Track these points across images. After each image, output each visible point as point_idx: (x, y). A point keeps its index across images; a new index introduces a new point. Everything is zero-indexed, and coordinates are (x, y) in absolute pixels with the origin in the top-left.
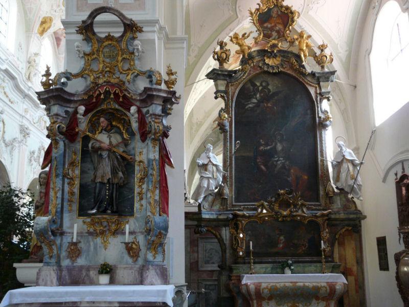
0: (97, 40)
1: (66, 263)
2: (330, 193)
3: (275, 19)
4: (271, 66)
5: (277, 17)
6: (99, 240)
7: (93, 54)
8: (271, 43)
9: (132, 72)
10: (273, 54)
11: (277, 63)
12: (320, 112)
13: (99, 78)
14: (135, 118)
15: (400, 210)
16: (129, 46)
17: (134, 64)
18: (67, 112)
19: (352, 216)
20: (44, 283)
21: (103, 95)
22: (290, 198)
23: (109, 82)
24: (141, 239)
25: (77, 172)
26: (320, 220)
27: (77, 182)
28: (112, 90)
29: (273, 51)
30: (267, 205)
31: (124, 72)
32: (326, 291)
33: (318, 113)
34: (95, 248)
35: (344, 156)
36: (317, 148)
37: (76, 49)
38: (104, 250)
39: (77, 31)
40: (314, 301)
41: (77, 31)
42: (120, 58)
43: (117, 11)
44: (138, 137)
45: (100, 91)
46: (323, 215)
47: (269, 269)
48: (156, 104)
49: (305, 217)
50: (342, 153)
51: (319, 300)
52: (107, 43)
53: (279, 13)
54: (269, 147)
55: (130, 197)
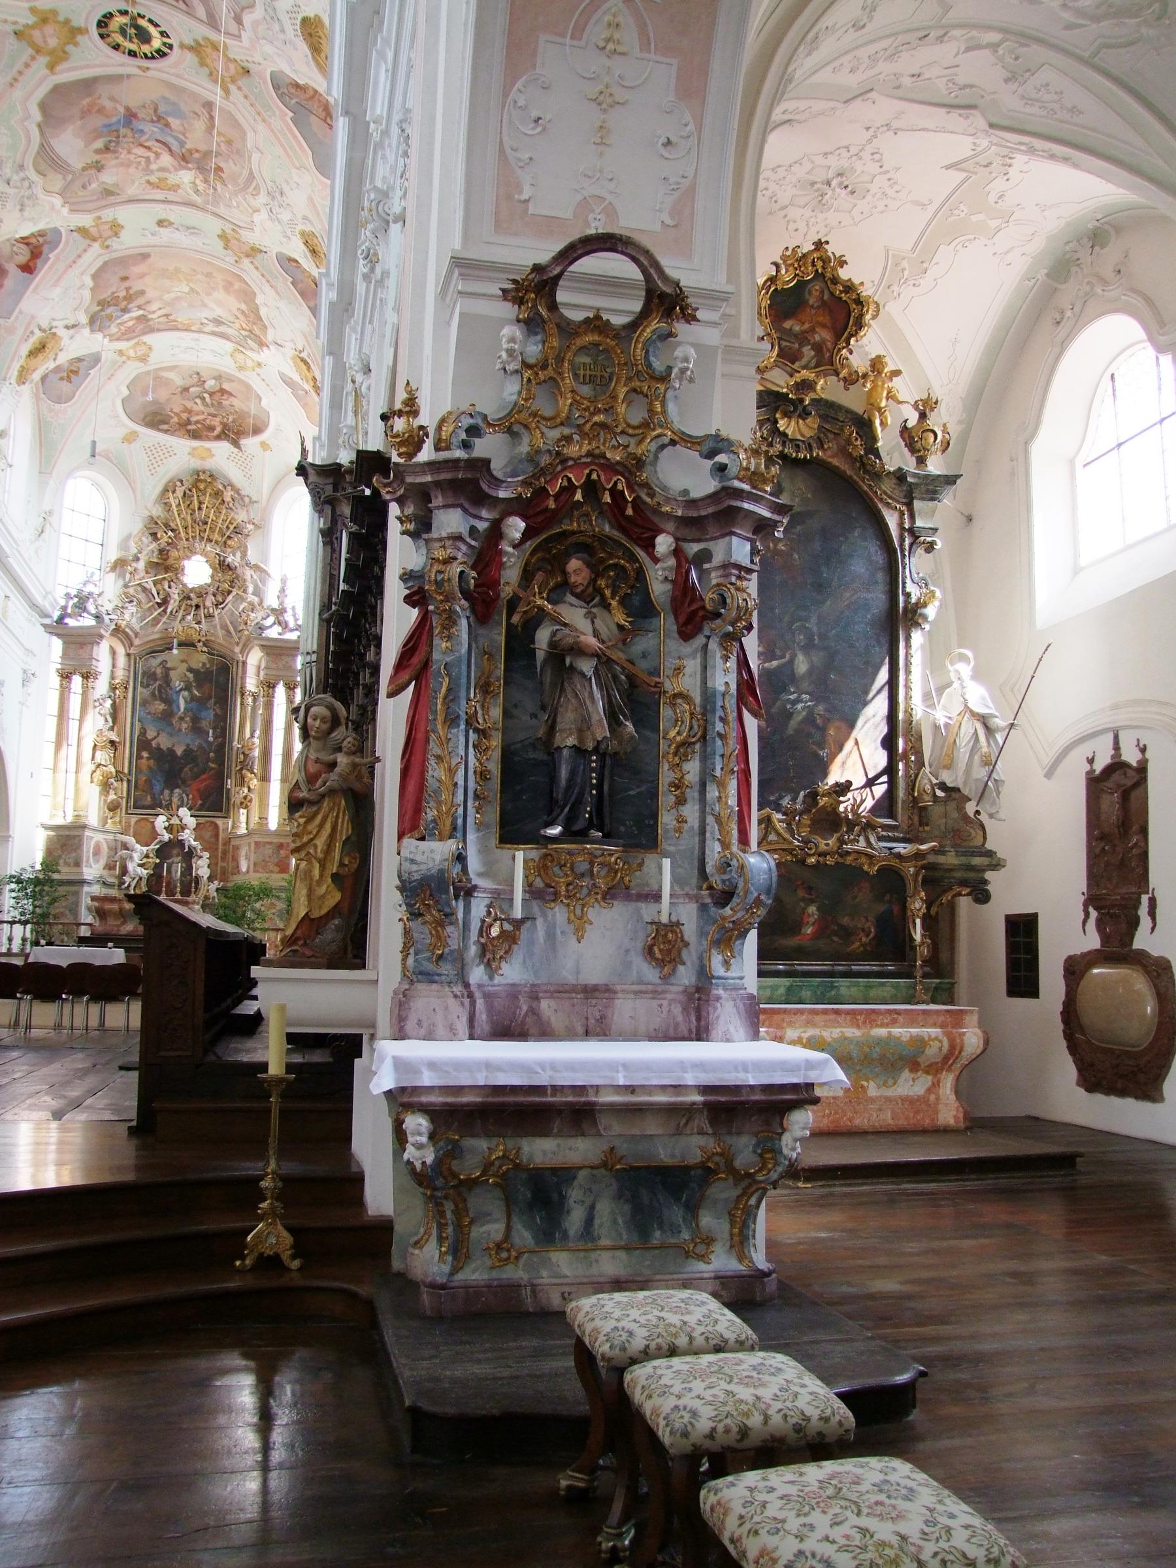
0: (558, 326)
1: (477, 974)
3: (813, 311)
4: (791, 440)
5: (819, 307)
6: (559, 914)
7: (544, 367)
8: (798, 377)
9: (654, 433)
10: (800, 408)
11: (808, 433)
13: (568, 439)
14: (664, 569)
15: (1098, 851)
16: (652, 359)
17: (664, 412)
18: (473, 530)
20: (423, 1032)
21: (579, 491)
23: (603, 456)
24: (688, 916)
25: (496, 713)
27: (496, 742)
28: (609, 481)
29: (802, 401)
30: (780, 821)
31: (631, 431)
32: (940, 1049)
34: (551, 935)
37: (505, 346)
38: (574, 940)
39: (504, 291)
40: (906, 1074)
41: (504, 291)
42: (622, 391)
43: (647, 252)
44: (666, 622)
45: (569, 480)
47: (782, 991)
48: (738, 535)
51: (917, 1071)
52: (588, 338)
53: (826, 297)
54: (775, 663)
55: (631, 793)
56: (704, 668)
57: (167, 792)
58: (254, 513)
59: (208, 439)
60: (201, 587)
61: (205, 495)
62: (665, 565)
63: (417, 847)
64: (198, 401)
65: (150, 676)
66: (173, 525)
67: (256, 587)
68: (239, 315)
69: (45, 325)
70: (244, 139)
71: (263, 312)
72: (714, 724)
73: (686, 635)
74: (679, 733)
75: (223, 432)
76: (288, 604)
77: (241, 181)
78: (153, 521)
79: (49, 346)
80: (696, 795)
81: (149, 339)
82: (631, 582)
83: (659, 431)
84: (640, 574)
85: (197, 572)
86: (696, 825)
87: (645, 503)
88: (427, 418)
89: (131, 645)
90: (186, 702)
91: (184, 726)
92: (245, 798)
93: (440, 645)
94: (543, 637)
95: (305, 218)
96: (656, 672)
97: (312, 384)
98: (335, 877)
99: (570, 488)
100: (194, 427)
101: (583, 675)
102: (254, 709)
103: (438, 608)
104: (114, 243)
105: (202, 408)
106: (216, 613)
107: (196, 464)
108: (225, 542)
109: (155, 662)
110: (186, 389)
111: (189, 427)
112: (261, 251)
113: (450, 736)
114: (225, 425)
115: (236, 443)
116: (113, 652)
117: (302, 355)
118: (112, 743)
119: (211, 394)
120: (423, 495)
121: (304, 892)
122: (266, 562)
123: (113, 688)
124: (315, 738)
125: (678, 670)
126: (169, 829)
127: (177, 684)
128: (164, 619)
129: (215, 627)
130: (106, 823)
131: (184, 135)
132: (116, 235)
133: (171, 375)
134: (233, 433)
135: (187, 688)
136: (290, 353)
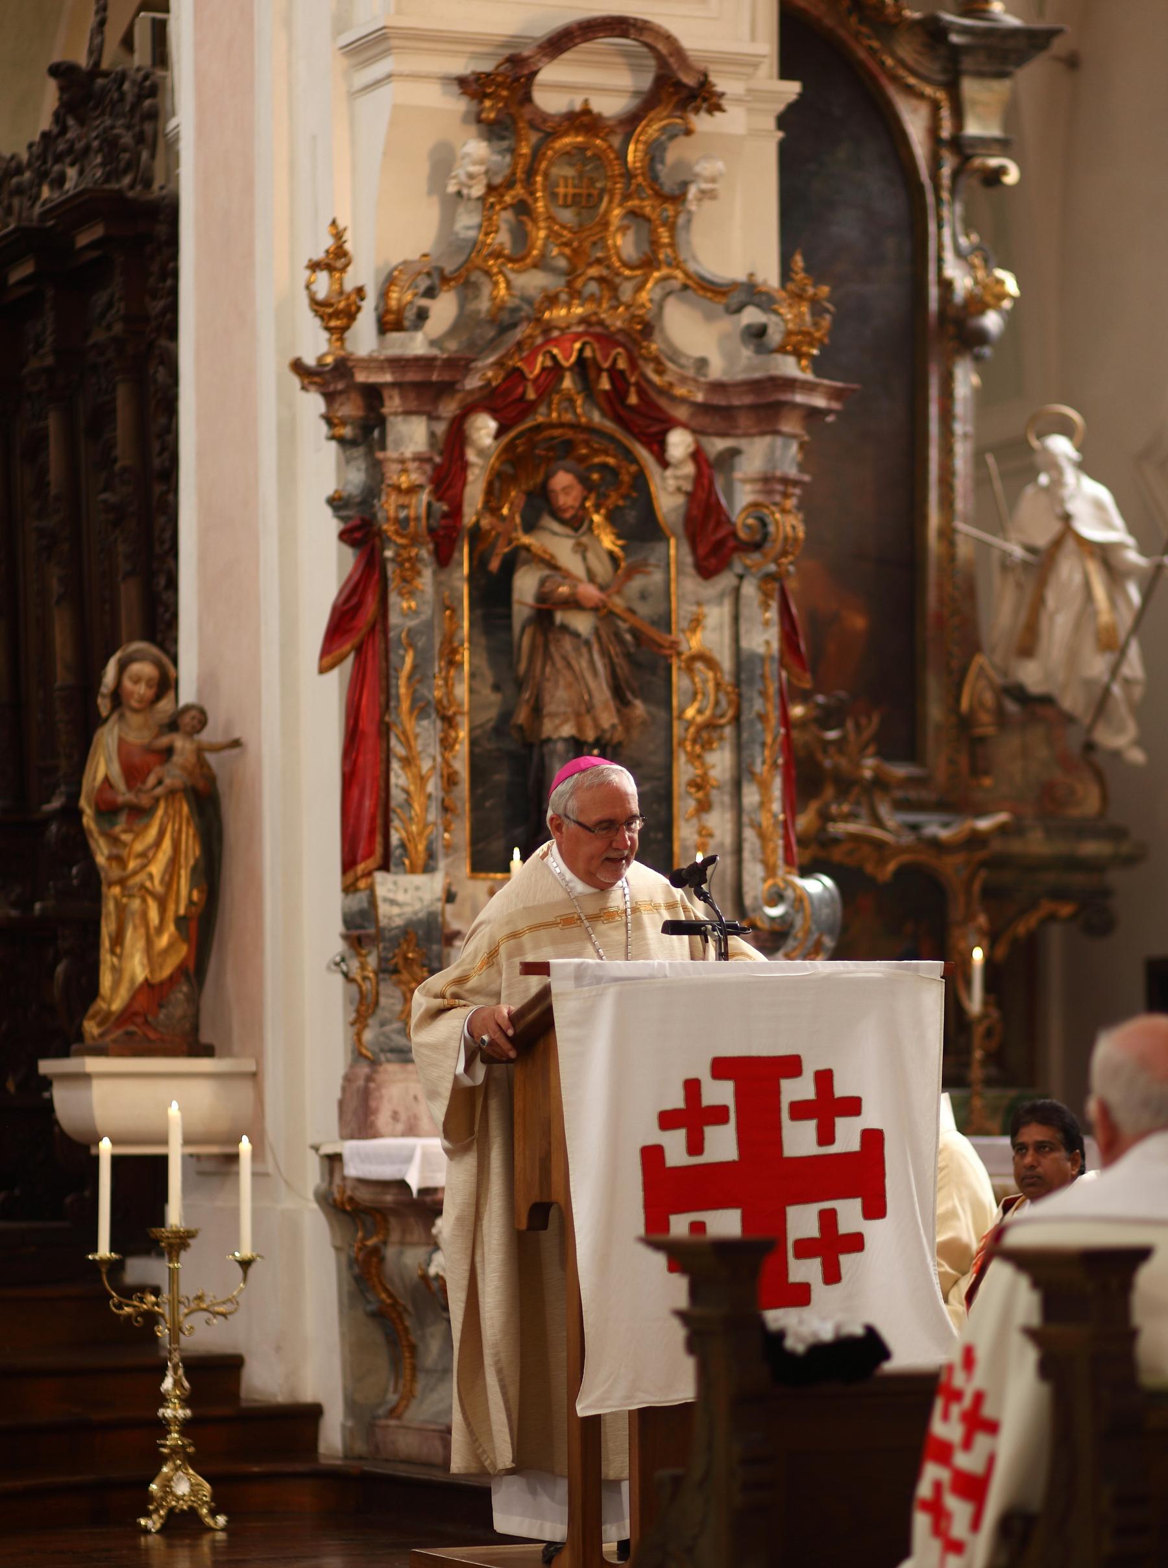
2: (985, 718)
12: (949, 255)
14: (677, 478)
17: (672, 245)
19: (1091, 848)
20: (400, 1127)
22: (826, 744)
26: (951, 867)
28: (606, 357)
33: (940, 260)
35: (1067, 518)
36: (925, 460)
44: (677, 550)
45: (554, 357)
46: (975, 840)
49: (879, 845)
50: (1061, 501)
56: (736, 619)
62: (680, 472)
63: (395, 883)
72: (751, 700)
73: (707, 570)
74: (700, 711)
80: (727, 799)
82: (624, 490)
83: (665, 271)
84: (641, 482)
86: (728, 840)
87: (649, 381)
88: (362, 273)
93: (399, 604)
94: (526, 585)
96: (665, 622)
98: (180, 921)
99: (555, 371)
101: (576, 635)
103: (397, 555)
113: (418, 730)
120: (373, 395)
121: (141, 944)
124: (136, 711)
125: (696, 623)
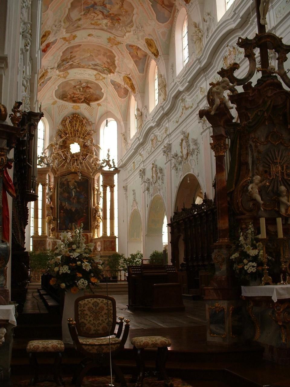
57: (70, 224)
58: (93, 128)
59: (79, 102)
60: (76, 153)
61: (77, 122)
64: (78, 90)
65: (62, 184)
66: (67, 132)
67: (96, 153)
68: (106, 63)
69: (46, 69)
70: (133, 11)
71: (116, 62)
75: (84, 100)
76: (111, 159)
77: (126, 23)
78: (60, 131)
79: (45, 75)
81: (69, 71)
85: (75, 148)
89: (56, 174)
90: (75, 193)
91: (75, 201)
92: (97, 225)
95: (149, 35)
97: (130, 85)
100: (75, 99)
102: (98, 195)
104: (72, 42)
105: (79, 92)
106: (83, 162)
107: (74, 111)
108: (84, 138)
109: (64, 180)
110: (75, 87)
111: (73, 99)
112: (121, 43)
114: (85, 98)
115: (89, 104)
116: (49, 177)
117: (129, 76)
118: (51, 208)
119: (83, 88)
122: (99, 143)
123: (50, 189)
126: (72, 237)
127: (72, 187)
128: (66, 165)
129: (83, 167)
130: (50, 235)
131: (110, 9)
132: (74, 39)
133: (72, 82)
134: (88, 101)
135: (75, 188)
136: (123, 75)
